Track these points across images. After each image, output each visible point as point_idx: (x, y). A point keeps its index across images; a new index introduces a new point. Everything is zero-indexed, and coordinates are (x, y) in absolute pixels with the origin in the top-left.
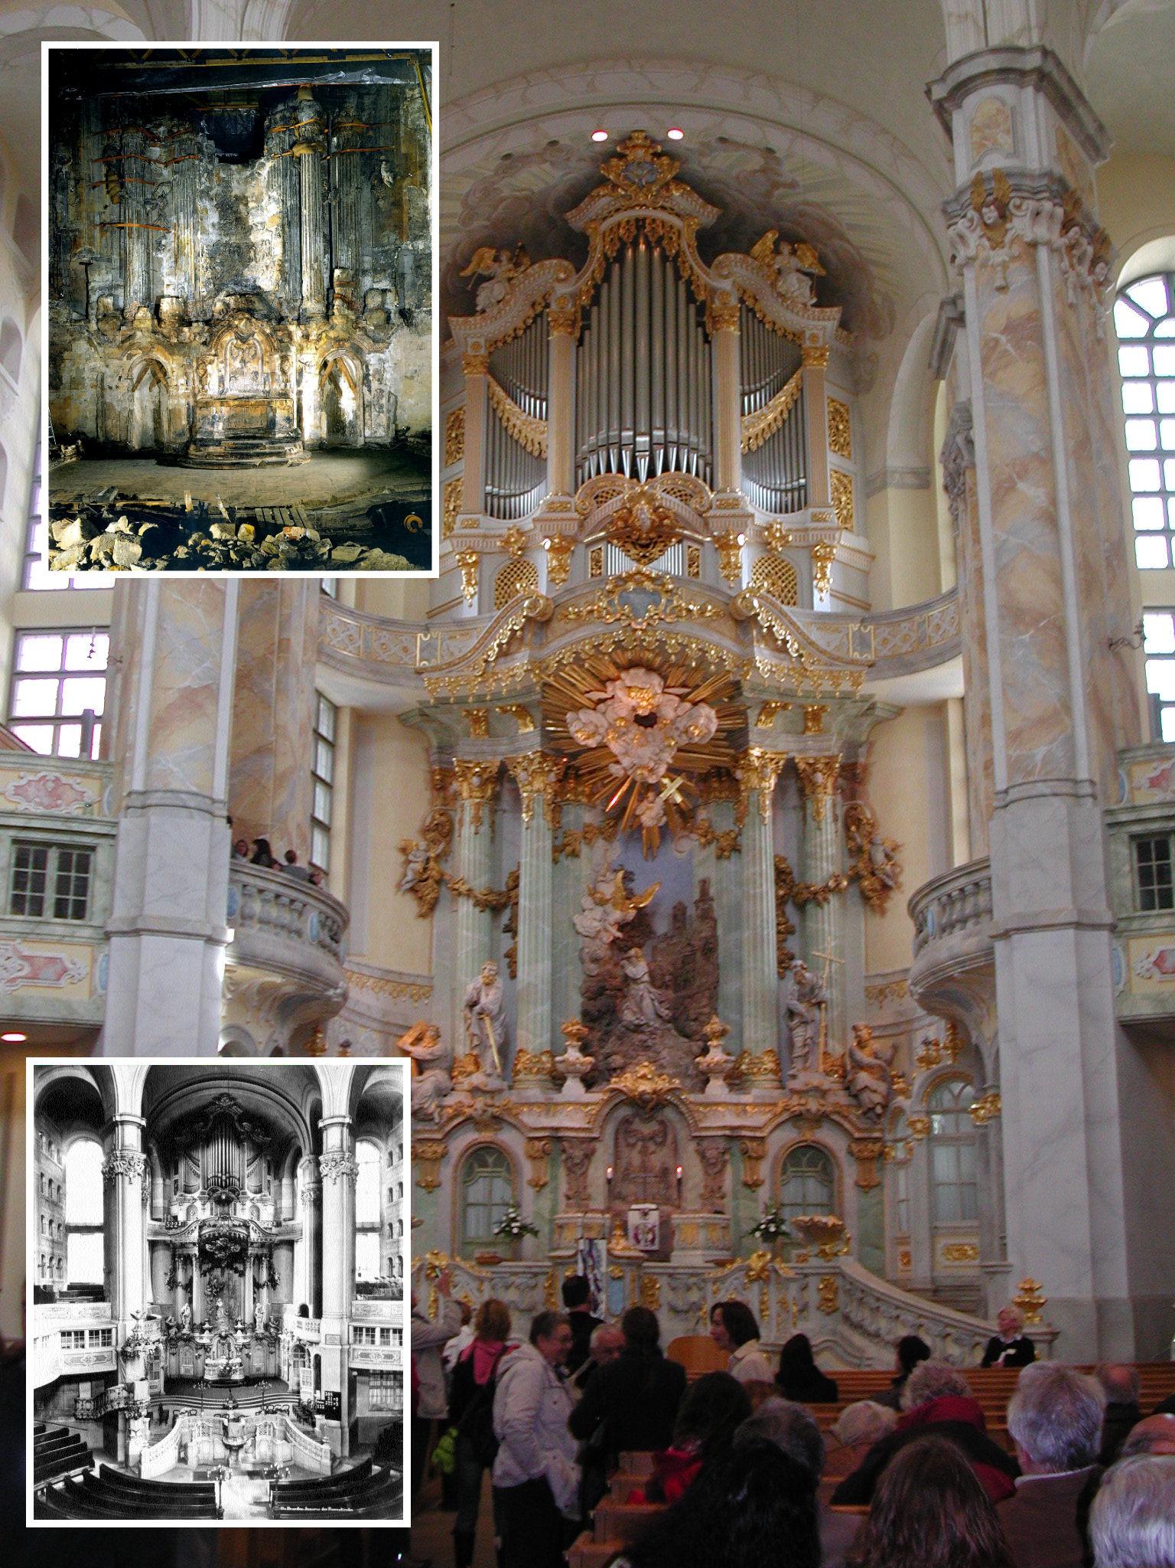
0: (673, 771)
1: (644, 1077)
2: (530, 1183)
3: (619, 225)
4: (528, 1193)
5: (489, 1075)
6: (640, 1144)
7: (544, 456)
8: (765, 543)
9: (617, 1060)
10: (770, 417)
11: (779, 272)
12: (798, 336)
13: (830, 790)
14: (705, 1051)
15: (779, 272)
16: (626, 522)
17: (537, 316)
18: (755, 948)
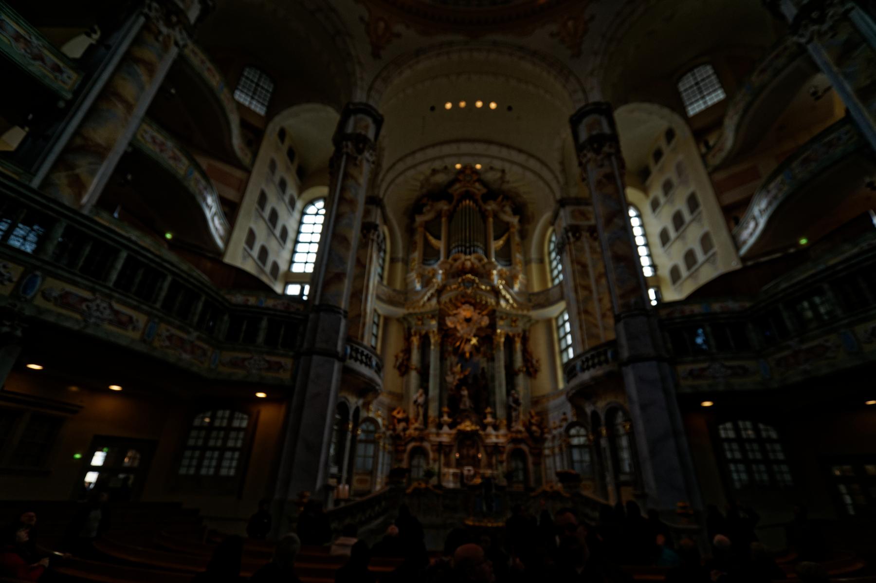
0: (475, 336)
9: (459, 420)
12: (508, 223)
14: (485, 418)
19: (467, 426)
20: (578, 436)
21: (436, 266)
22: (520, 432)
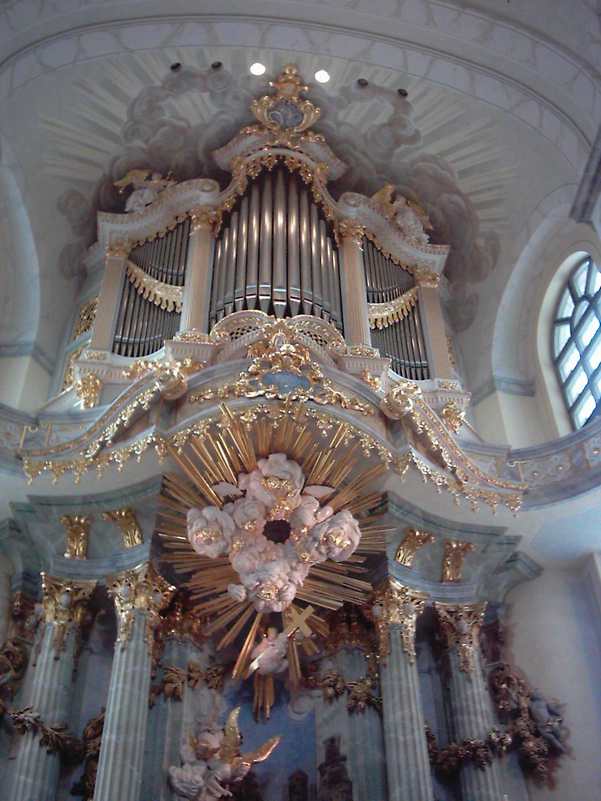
3: (262, 159)
7: (177, 311)
15: (396, 214)
17: (178, 225)
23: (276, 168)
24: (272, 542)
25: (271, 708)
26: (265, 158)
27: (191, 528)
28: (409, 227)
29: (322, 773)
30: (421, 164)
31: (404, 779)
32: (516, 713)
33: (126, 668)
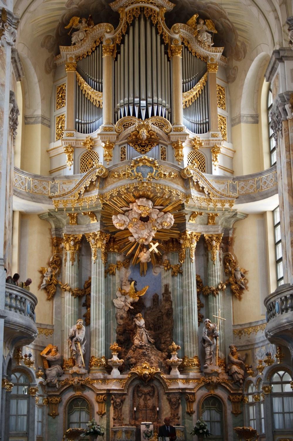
0: (154, 240)
1: (145, 368)
2: (97, 413)
3: (133, 9)
4: (97, 418)
5: (80, 367)
6: (143, 396)
7: (101, 107)
8: (193, 147)
9: (133, 360)
10: (195, 93)
11: (199, 32)
12: (206, 58)
13: (218, 248)
14: (169, 357)
16: (136, 136)
17: (97, 47)
18: (189, 313)
19: (146, 369)
20: (282, 383)
21: (94, 135)
22: (217, 374)
23: (140, 16)
24: (143, 222)
25: (146, 271)
26: (135, 10)
27: (114, 221)
28: (204, 41)
29: (163, 296)
30: (211, 5)
31: (187, 304)
32: (230, 272)
33: (96, 270)
